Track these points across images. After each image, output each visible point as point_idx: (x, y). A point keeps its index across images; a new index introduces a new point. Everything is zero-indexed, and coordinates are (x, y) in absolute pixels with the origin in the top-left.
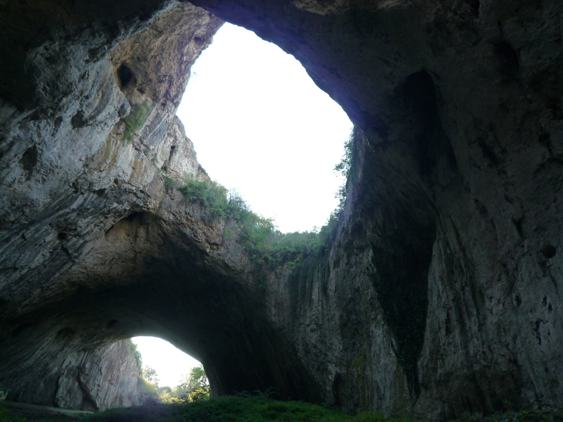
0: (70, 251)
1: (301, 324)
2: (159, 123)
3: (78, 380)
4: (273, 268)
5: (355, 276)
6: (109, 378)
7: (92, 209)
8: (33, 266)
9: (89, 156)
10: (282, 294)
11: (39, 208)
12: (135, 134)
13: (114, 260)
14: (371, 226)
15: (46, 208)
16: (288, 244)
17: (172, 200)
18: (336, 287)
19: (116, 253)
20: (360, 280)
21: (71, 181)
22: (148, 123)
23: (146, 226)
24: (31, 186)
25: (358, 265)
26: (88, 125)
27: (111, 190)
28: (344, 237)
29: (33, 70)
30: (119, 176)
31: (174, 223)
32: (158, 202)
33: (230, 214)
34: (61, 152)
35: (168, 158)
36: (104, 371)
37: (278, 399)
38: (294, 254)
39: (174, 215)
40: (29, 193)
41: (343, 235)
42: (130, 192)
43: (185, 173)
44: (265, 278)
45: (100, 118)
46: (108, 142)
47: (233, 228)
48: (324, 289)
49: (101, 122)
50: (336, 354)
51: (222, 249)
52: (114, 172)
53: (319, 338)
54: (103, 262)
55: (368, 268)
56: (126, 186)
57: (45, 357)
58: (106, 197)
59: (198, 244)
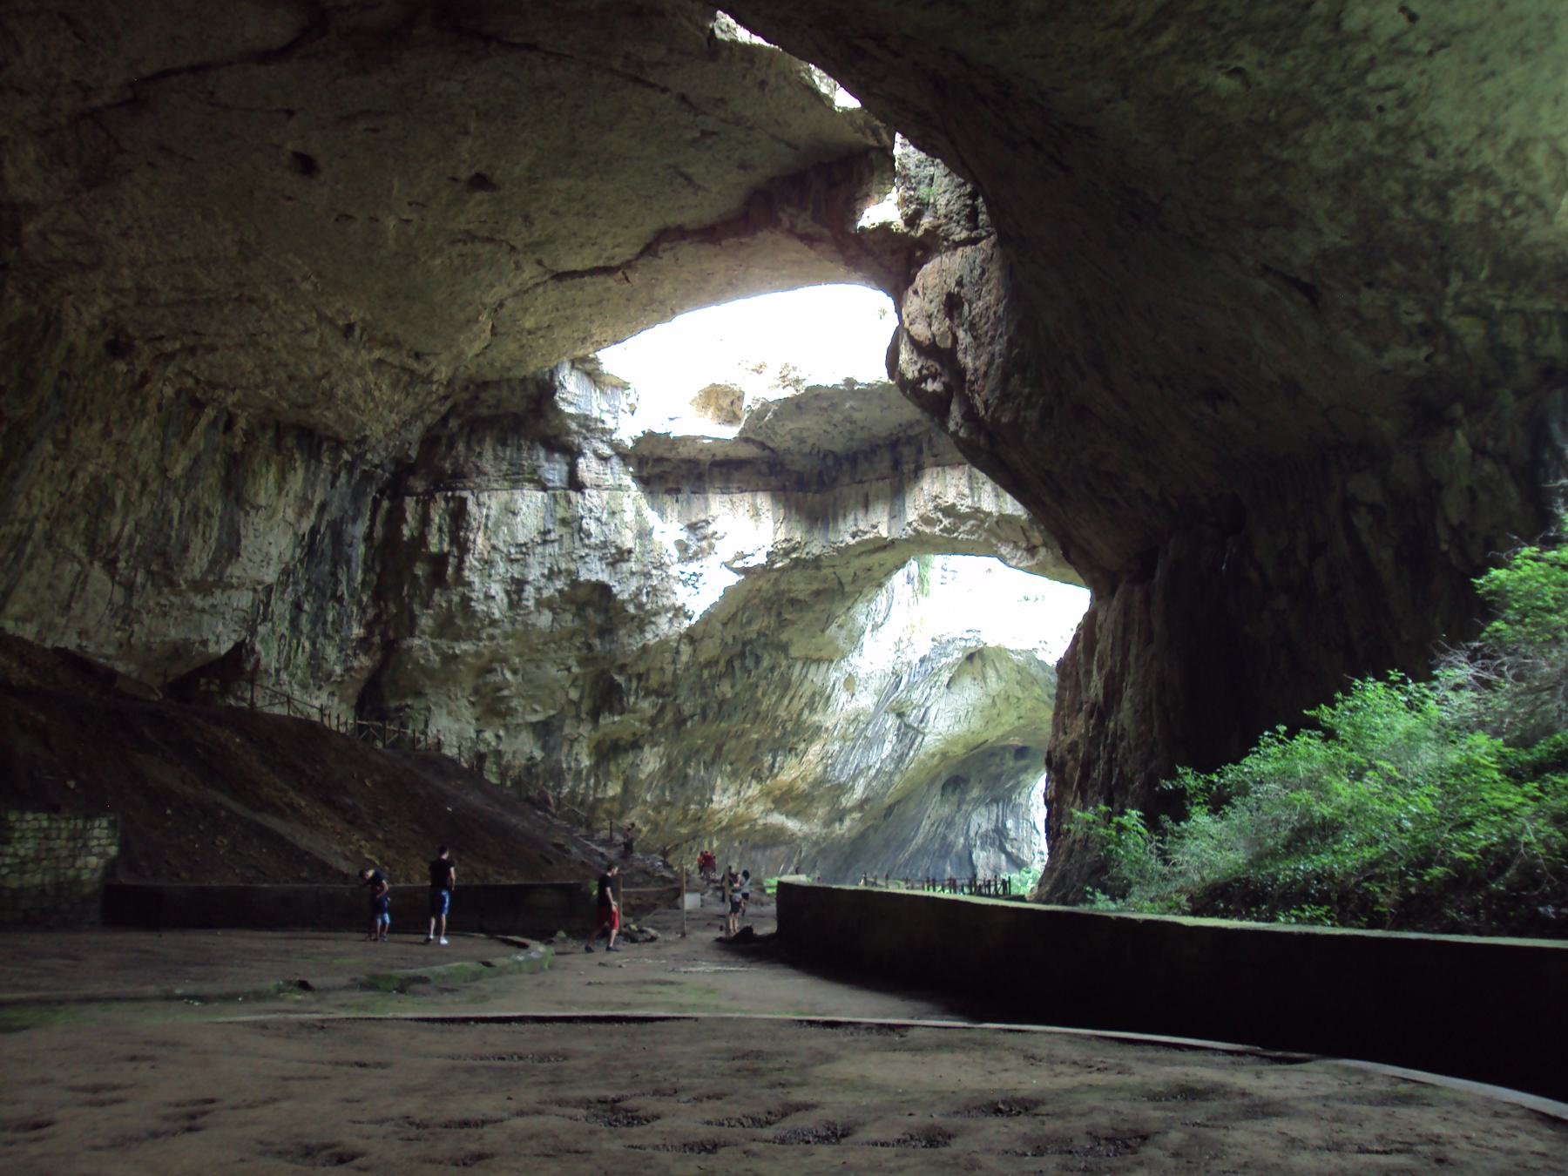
3: (1003, 850)
29: (832, 641)
58: (930, 659)
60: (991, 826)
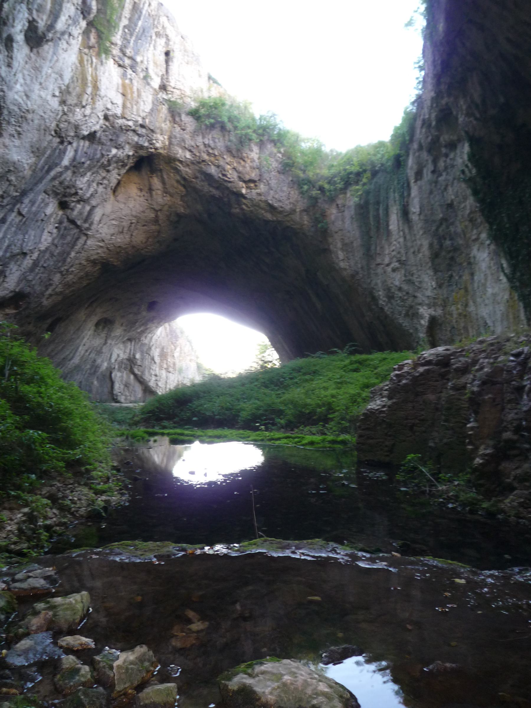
0: (79, 223)
1: (379, 264)
2: (139, 18)
4: (332, 200)
5: (447, 186)
6: (165, 366)
7: (88, 162)
8: (43, 248)
9: (63, 87)
10: (349, 232)
11: (26, 172)
12: (112, 44)
13: (133, 225)
14: (464, 107)
15: (34, 171)
16: (349, 161)
17: (184, 130)
18: (420, 208)
19: (132, 215)
20: (453, 190)
21: (51, 128)
22: (124, 22)
23: (159, 174)
24: (7, 144)
25: (449, 171)
26: (48, 41)
27: (104, 131)
28: (426, 133)
30: (108, 109)
31: (193, 163)
32: (166, 137)
33: (263, 135)
34: (26, 88)
35: (164, 70)
36: (157, 359)
37: (361, 353)
38: (358, 174)
39: (190, 151)
40: (8, 154)
41: (424, 130)
42: (128, 129)
43: (191, 90)
44: (324, 215)
45: (60, 25)
46: (81, 62)
47: (271, 155)
48: (405, 213)
49: (63, 33)
50: (429, 293)
51: (262, 186)
52: (100, 105)
53: (403, 278)
54: (121, 230)
55: (463, 172)
56: (120, 122)
57: (91, 352)
58: (100, 143)
59: (229, 185)
60: (126, 356)
